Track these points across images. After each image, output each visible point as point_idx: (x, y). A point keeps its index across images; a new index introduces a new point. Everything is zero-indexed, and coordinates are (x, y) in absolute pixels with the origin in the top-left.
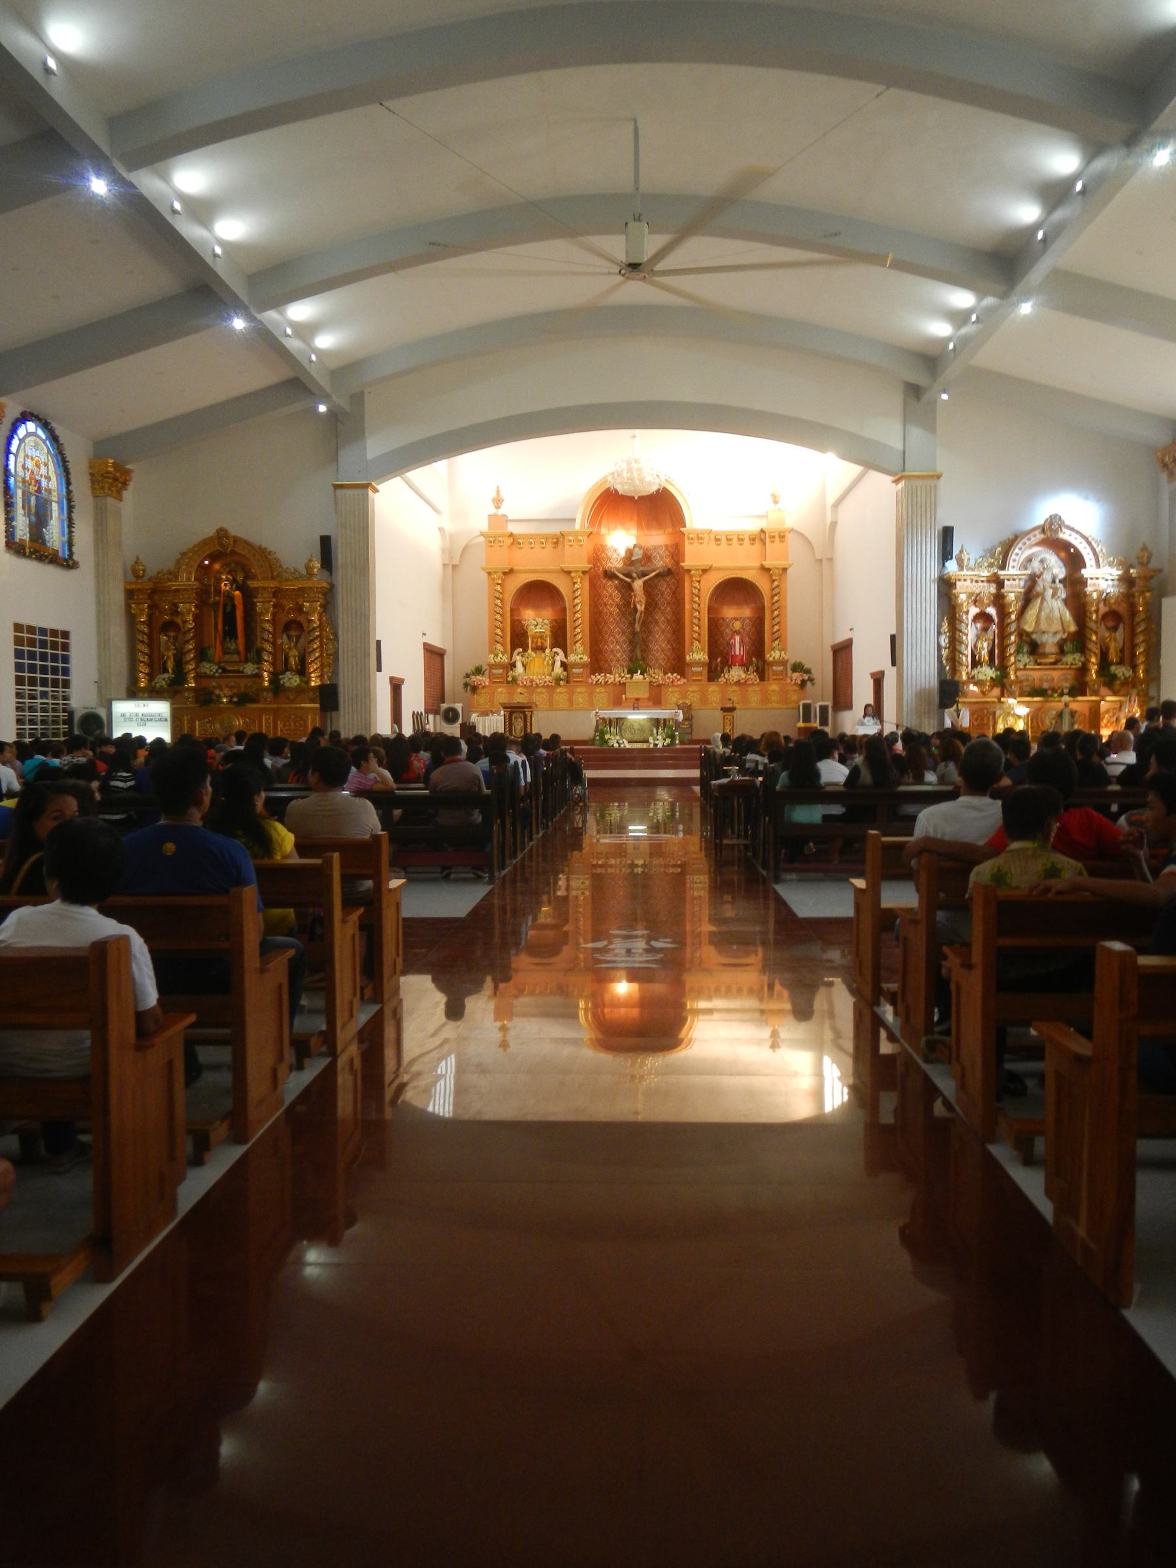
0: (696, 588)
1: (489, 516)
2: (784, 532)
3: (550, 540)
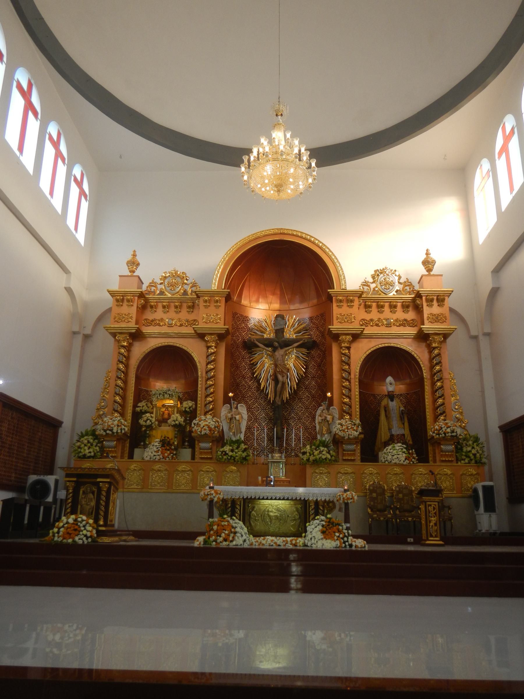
0: (344, 354)
1: (120, 276)
2: (443, 296)
3: (185, 305)
